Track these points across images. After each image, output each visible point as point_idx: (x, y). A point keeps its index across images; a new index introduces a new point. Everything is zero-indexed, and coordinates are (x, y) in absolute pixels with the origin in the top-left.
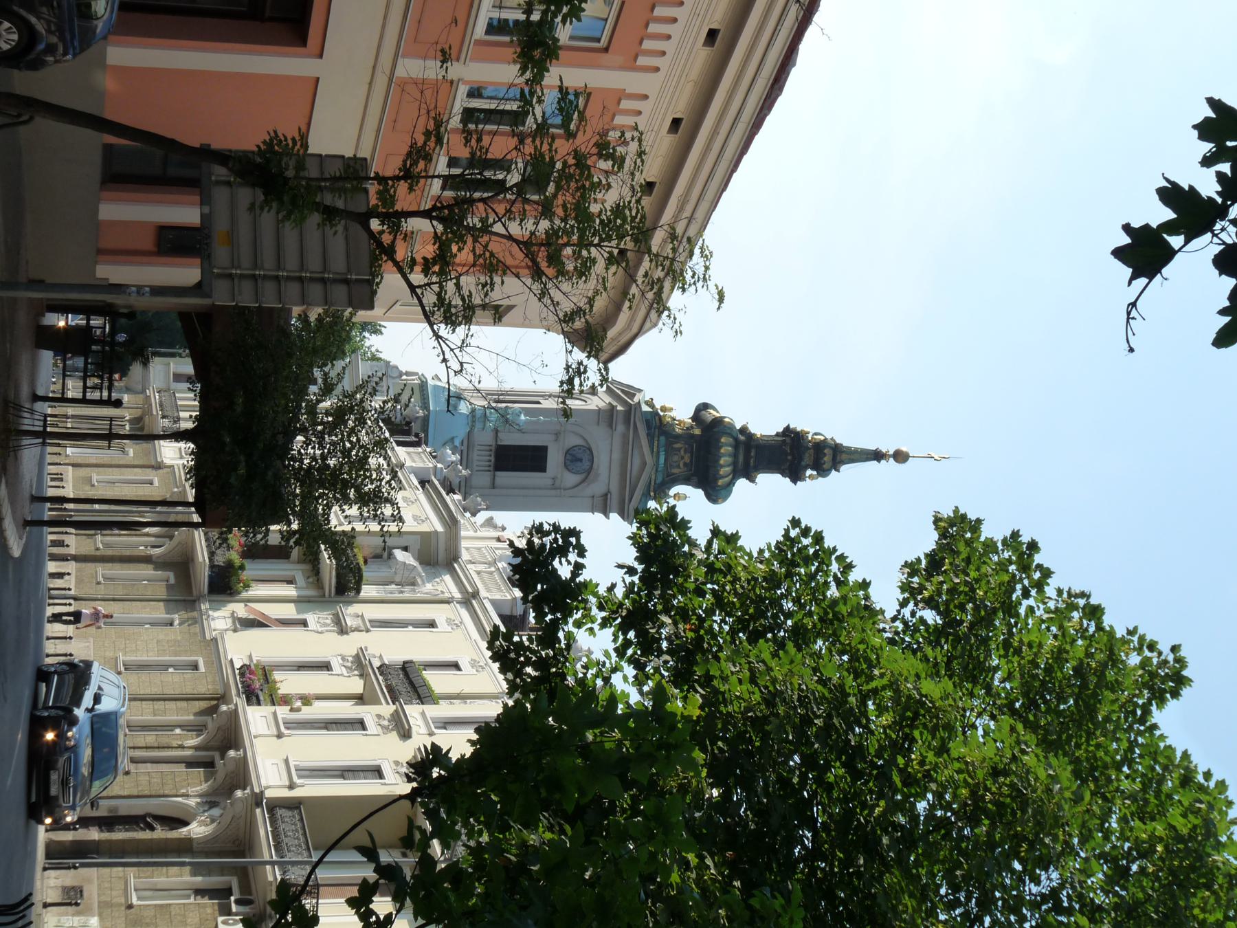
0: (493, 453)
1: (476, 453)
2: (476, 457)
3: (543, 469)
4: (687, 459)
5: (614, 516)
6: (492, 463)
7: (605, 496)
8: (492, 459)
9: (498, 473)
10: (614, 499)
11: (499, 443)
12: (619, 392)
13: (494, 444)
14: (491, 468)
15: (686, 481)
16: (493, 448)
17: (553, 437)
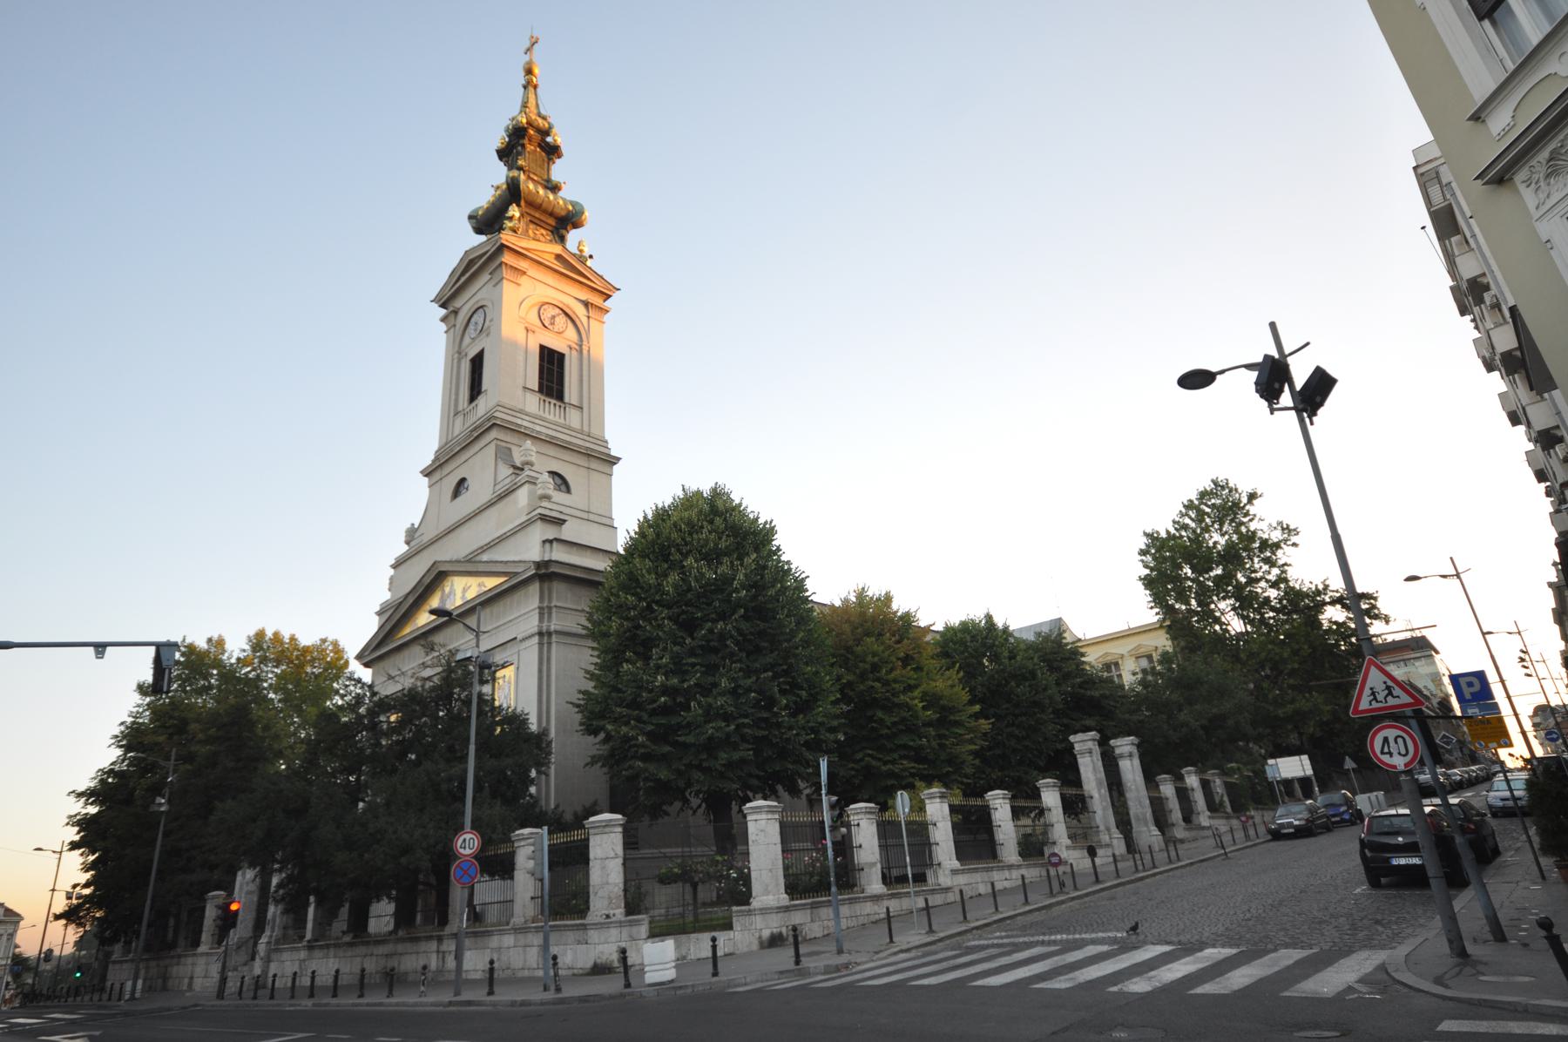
0: (548, 400)
1: (546, 415)
2: (551, 417)
3: (561, 356)
4: (544, 232)
5: (608, 304)
6: (558, 403)
7: (586, 304)
8: (553, 401)
9: (567, 399)
10: (596, 300)
11: (537, 389)
12: (463, 279)
13: (538, 394)
14: (563, 405)
15: (562, 239)
16: (543, 398)
17: (530, 334)
